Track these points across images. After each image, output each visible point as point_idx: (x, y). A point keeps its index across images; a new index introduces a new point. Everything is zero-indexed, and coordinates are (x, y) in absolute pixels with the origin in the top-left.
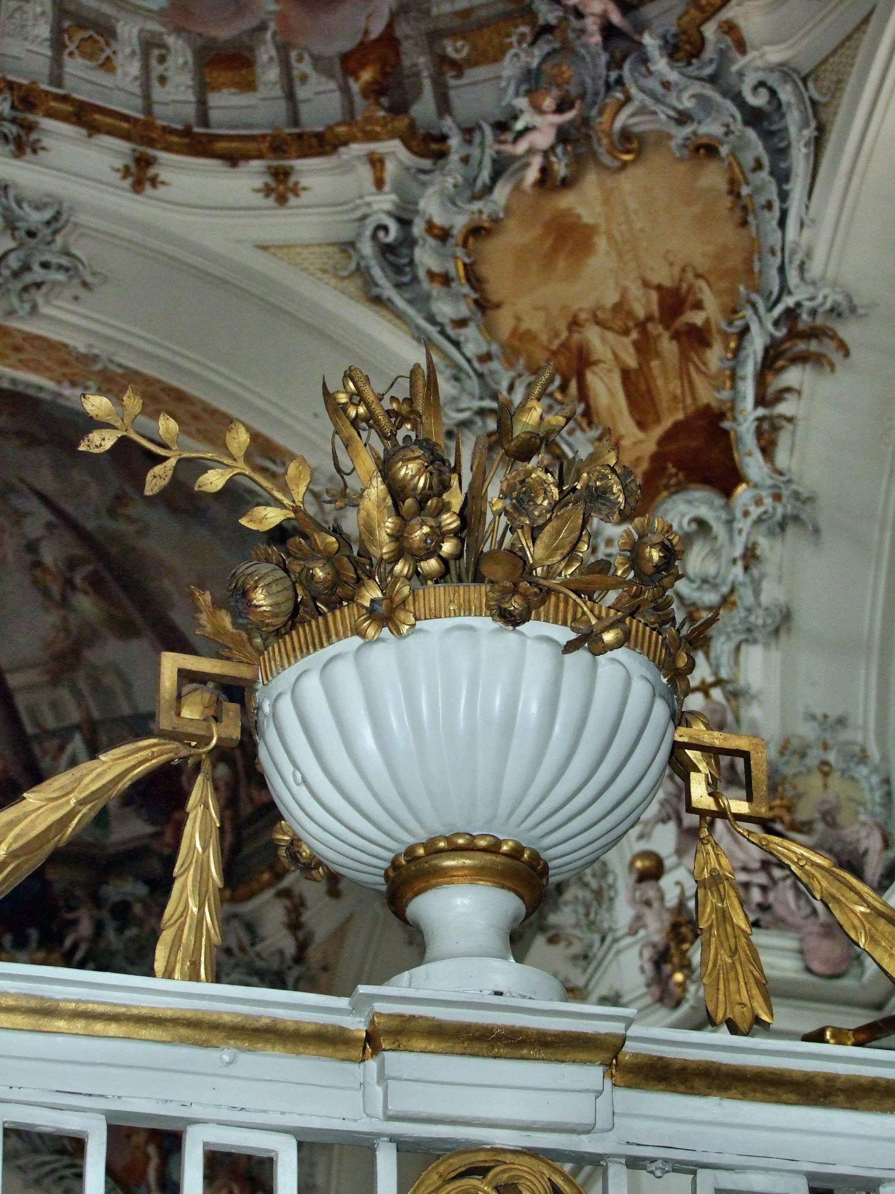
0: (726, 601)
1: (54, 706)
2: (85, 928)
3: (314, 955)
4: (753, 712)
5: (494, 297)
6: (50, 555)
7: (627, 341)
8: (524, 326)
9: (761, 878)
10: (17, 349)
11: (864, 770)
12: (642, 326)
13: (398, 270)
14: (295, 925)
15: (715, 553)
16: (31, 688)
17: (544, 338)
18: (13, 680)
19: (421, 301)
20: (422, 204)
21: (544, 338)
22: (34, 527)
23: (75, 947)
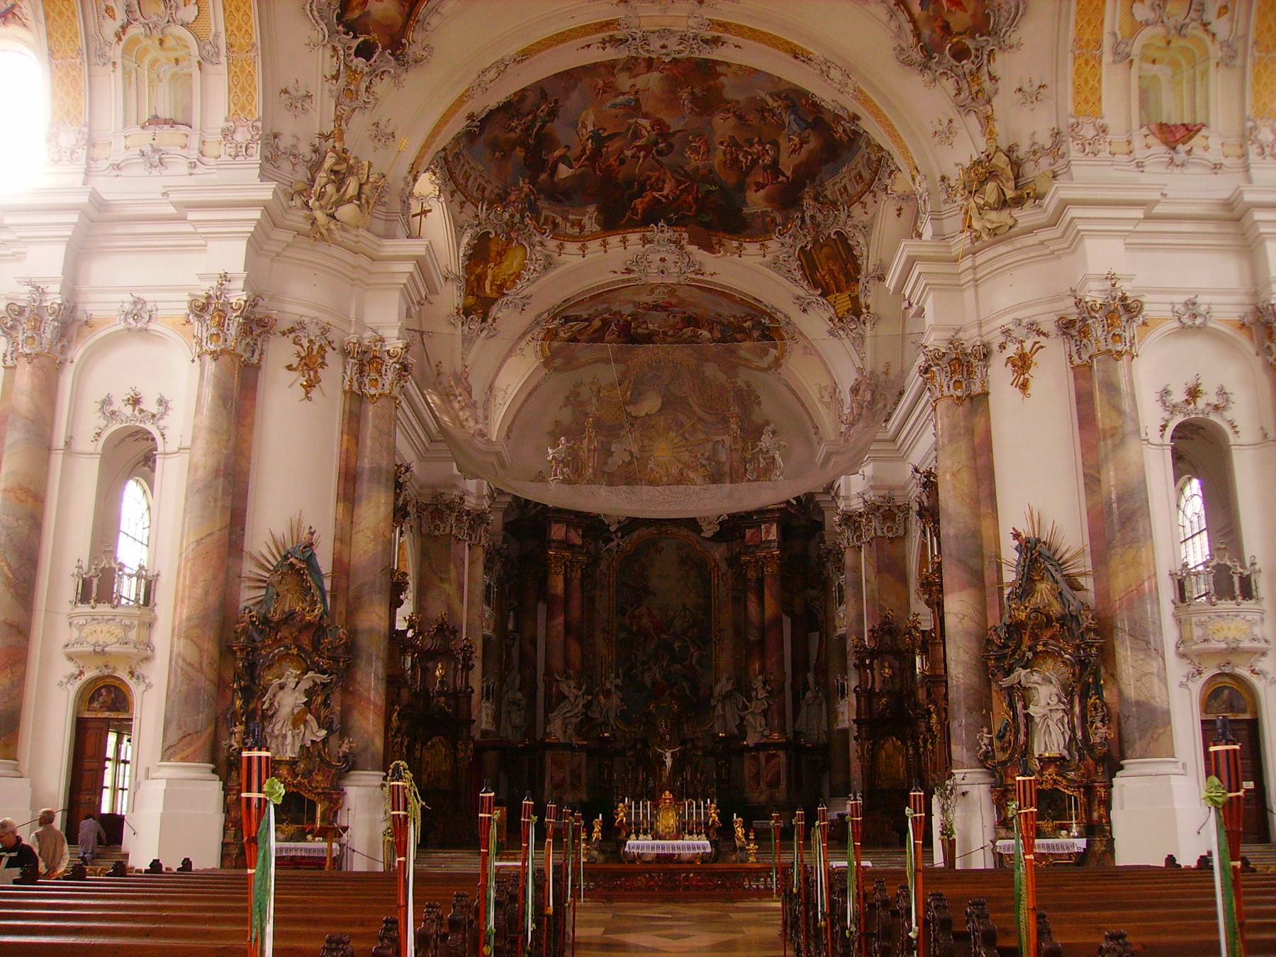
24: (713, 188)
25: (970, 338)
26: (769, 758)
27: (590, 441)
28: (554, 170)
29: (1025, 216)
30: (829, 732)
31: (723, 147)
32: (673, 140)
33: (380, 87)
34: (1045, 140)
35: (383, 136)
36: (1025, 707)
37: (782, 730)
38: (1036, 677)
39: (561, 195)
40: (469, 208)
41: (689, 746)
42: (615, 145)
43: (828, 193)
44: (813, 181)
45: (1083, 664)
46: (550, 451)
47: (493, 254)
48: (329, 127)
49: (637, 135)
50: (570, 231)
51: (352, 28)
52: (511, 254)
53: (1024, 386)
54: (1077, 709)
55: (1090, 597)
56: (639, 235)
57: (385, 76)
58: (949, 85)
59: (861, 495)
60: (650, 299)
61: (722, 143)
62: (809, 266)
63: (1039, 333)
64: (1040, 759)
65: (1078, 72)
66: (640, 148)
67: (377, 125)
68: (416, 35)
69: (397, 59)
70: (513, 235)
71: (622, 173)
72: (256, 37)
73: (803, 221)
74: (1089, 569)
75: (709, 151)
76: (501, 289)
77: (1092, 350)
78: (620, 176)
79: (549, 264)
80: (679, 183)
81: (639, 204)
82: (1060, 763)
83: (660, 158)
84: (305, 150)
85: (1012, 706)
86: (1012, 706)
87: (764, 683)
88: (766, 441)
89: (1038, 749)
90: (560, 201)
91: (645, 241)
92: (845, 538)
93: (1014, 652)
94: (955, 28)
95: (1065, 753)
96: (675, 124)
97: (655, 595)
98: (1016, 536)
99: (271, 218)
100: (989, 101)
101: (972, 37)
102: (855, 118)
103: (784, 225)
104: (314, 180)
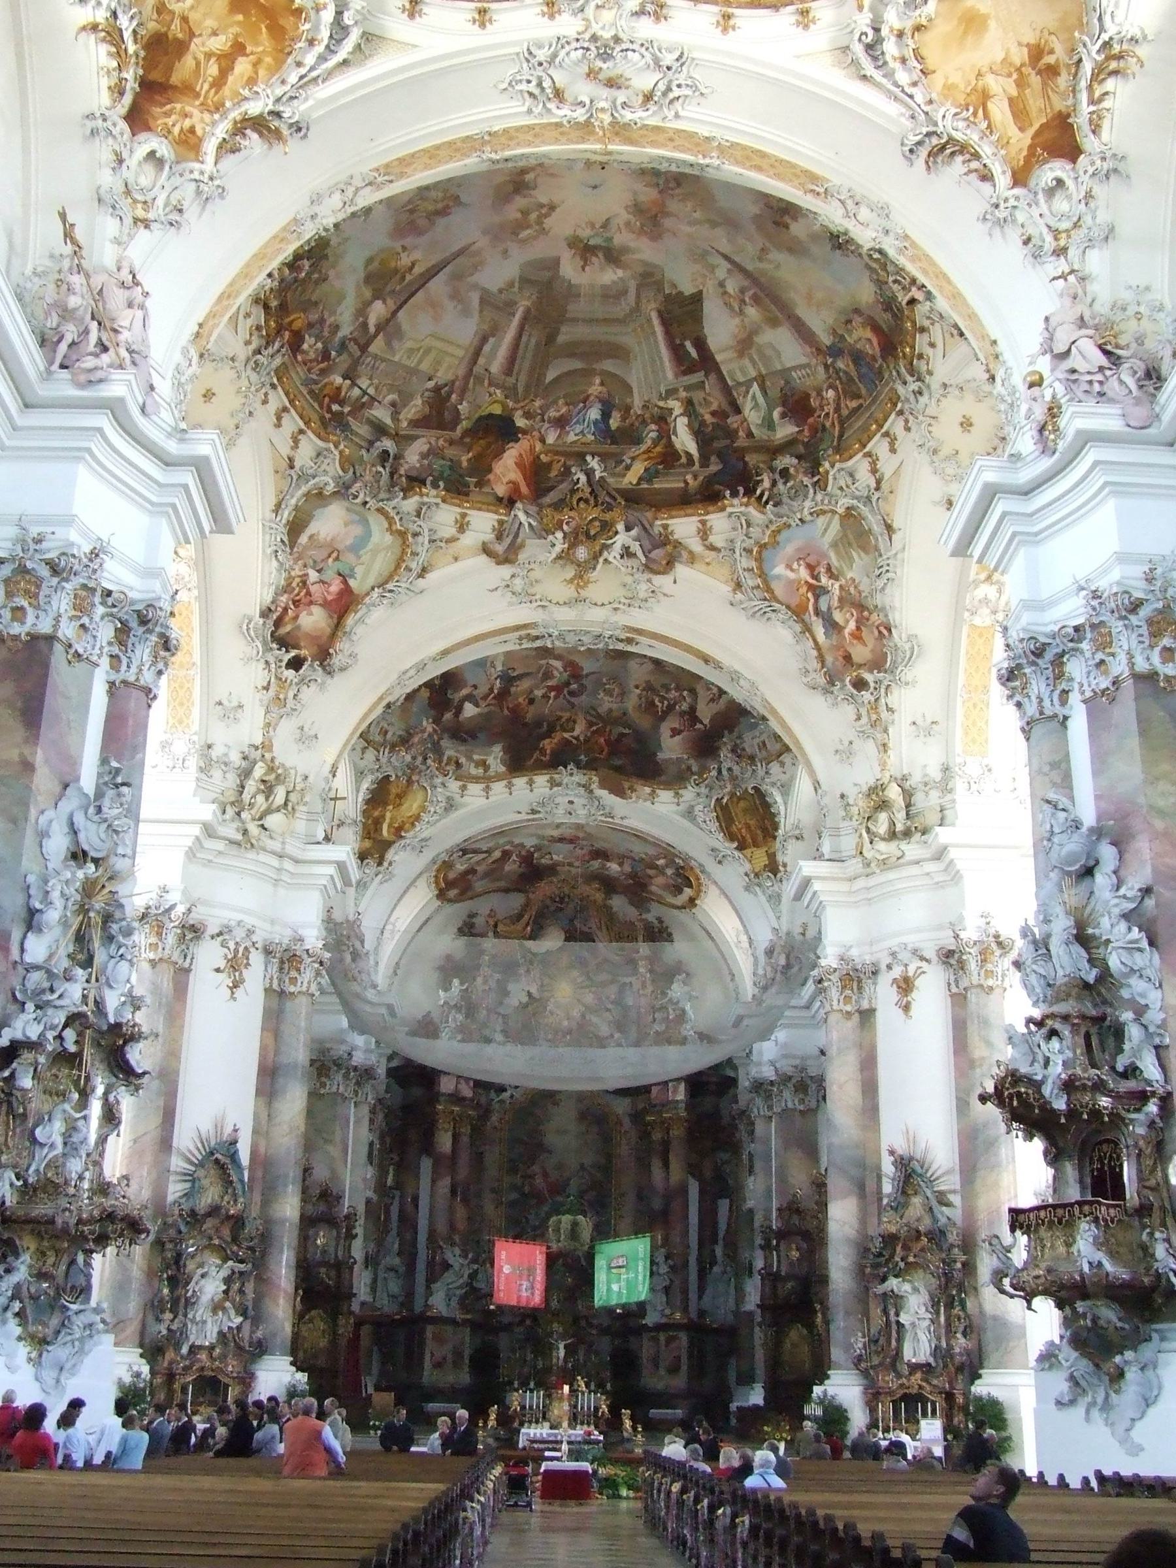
0: (1076, 225)
1: (742, 370)
2: (767, 484)
3: (884, 485)
4: (1093, 288)
5: (931, 68)
6: (731, 287)
7: (1011, 80)
8: (950, 81)
9: (1099, 377)
10: (671, 140)
11: (1162, 315)
12: (1019, 70)
13: (875, 58)
14: (874, 471)
15: (1069, 198)
16: (731, 360)
17: (962, 86)
18: (719, 358)
19: (890, 75)
20: (886, 16)
21: (962, 86)
22: (721, 273)
23: (762, 494)
24: (627, 731)
25: (861, 955)
26: (669, 1340)
27: (485, 982)
28: (459, 709)
29: (912, 849)
30: (737, 1313)
31: (638, 691)
32: (584, 682)
33: (307, 693)
34: (935, 774)
35: (306, 738)
36: (897, 1315)
37: (685, 1310)
38: (907, 1287)
39: (463, 734)
40: (371, 754)
41: (583, 1323)
42: (525, 684)
43: (746, 745)
44: (731, 732)
45: (948, 1277)
46: (441, 993)
47: (392, 797)
48: (258, 740)
49: (547, 675)
50: (474, 771)
51: (284, 643)
52: (410, 797)
53: (906, 1008)
54: (942, 1319)
55: (955, 1213)
56: (547, 777)
57: (312, 684)
58: (849, 710)
59: (772, 1063)
60: (556, 833)
61: (637, 687)
62: (725, 816)
63: (922, 959)
64: (909, 1365)
65: (967, 717)
66: (551, 689)
67: (302, 728)
68: (342, 646)
69: (324, 669)
70: (414, 778)
71: (531, 714)
72: (197, 657)
73: (720, 772)
74: (958, 1187)
75: (623, 694)
76: (398, 832)
77: (964, 983)
78: (529, 716)
79: (450, 806)
80: (591, 724)
81: (548, 744)
82: (926, 1368)
83: (573, 700)
84: (235, 758)
85: (885, 1312)
86: (885, 1312)
87: (667, 1258)
88: (677, 990)
89: (908, 1354)
90: (464, 741)
91: (553, 784)
92: (759, 1107)
93: (888, 1261)
94: (856, 658)
95: (931, 1360)
96: (587, 666)
97: (550, 1152)
98: (892, 1153)
99: (209, 831)
100: (886, 731)
101: (871, 672)
102: (764, 719)
103: (700, 774)
104: (243, 787)
